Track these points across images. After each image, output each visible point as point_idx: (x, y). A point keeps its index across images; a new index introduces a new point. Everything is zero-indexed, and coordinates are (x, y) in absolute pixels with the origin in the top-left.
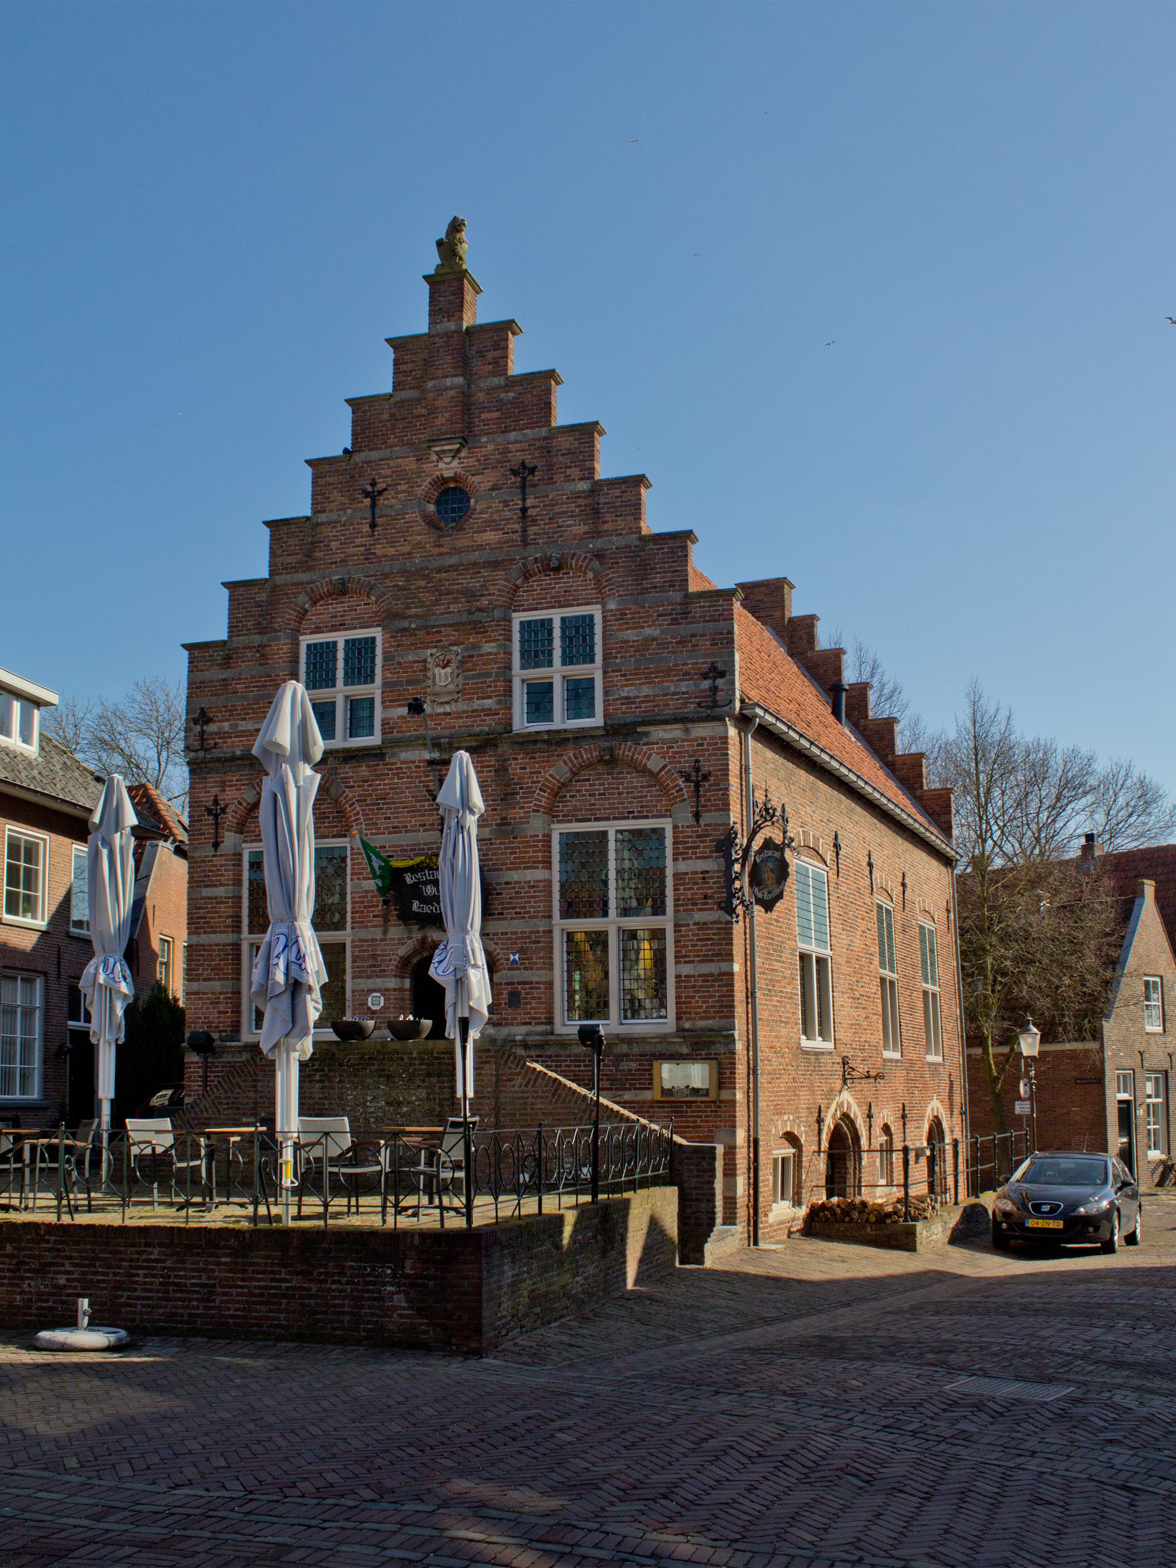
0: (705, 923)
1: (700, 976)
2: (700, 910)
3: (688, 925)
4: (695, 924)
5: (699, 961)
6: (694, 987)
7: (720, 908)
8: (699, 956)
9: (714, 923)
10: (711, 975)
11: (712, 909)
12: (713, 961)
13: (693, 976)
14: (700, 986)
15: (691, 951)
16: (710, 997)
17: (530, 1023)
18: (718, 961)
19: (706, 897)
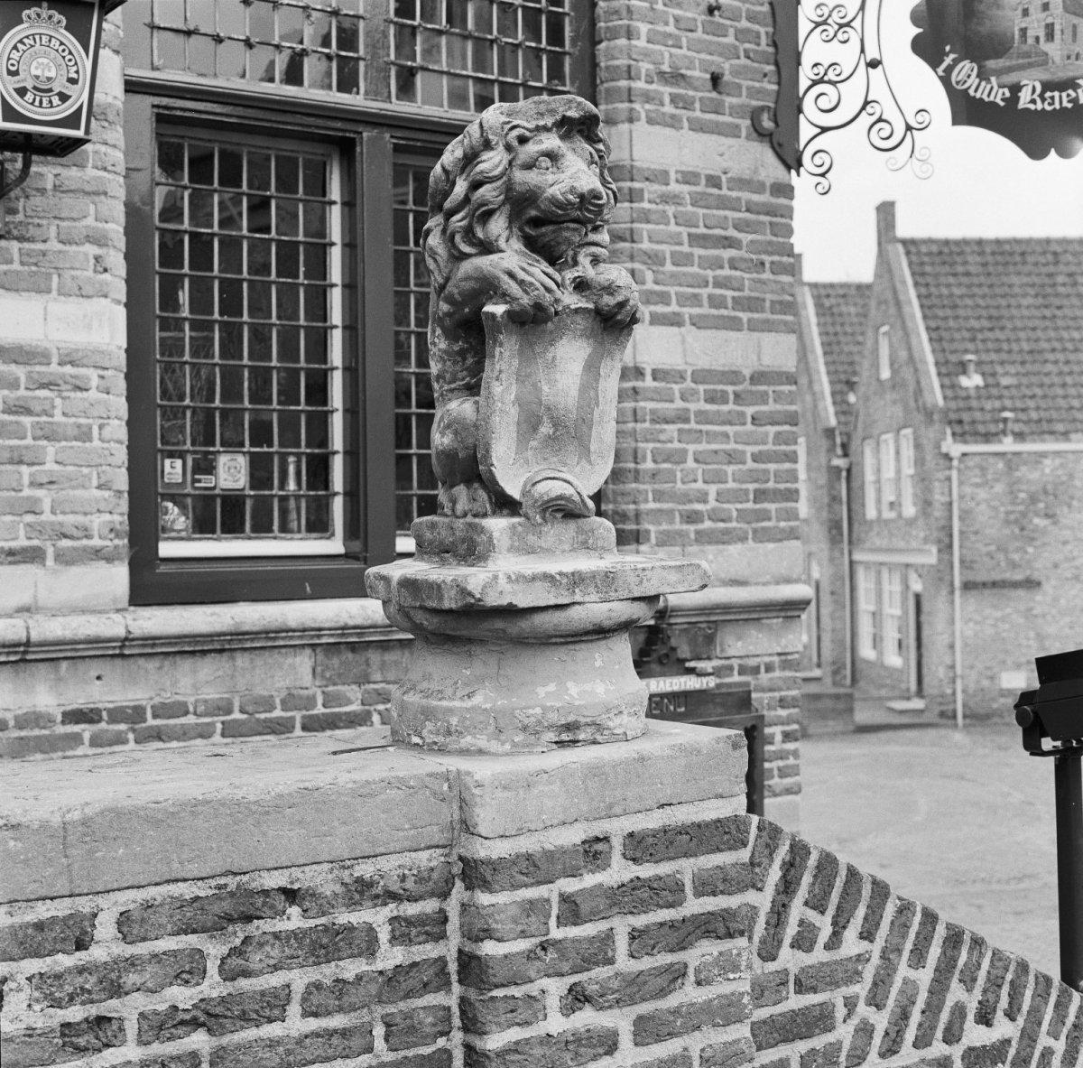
0: (714, 181)
1: (700, 376)
2: (698, 127)
3: (661, 177)
4: (688, 178)
5: (698, 323)
6: (682, 417)
7: (760, 134)
8: (695, 300)
9: (741, 183)
10: (733, 376)
11: (733, 131)
12: (734, 324)
13: (681, 376)
14: (703, 417)
15: (675, 279)
16: (732, 458)
17: (32, 556)
18: (753, 327)
19: (716, 80)
